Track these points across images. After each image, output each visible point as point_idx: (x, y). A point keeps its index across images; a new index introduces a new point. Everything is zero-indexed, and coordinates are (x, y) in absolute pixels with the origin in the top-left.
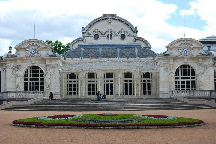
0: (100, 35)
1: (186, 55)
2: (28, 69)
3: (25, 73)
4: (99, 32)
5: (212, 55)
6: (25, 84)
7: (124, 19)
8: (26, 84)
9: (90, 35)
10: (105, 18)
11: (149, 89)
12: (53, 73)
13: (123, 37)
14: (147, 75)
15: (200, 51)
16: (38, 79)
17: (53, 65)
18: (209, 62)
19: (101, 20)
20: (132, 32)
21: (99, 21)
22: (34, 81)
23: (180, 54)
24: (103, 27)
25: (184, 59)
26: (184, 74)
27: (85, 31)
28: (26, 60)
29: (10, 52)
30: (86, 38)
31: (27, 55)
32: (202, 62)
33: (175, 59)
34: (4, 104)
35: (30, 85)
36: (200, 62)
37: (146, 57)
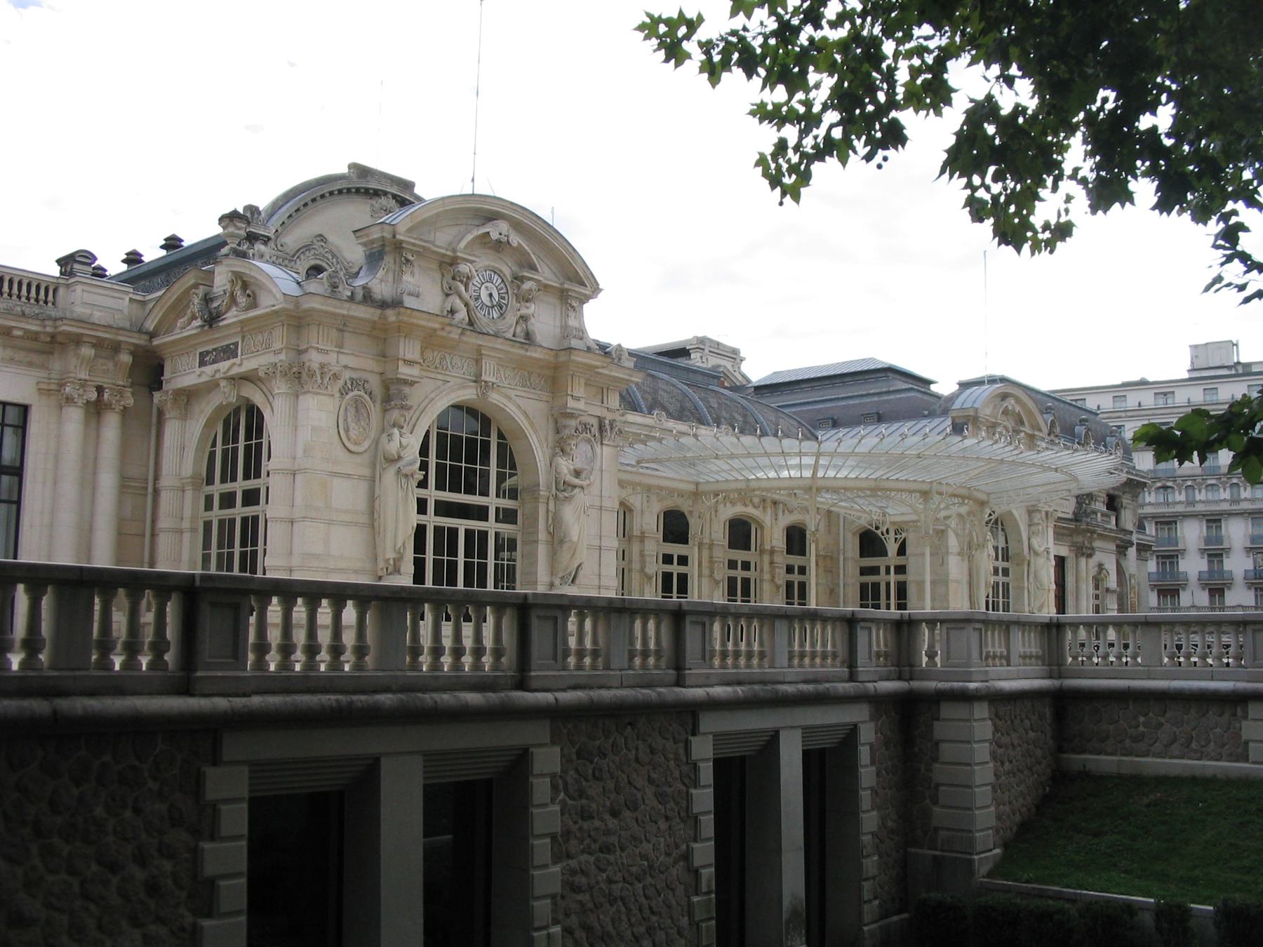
4: (334, 256)
16: (481, 513)
19: (349, 190)
21: (340, 192)
22: (462, 525)
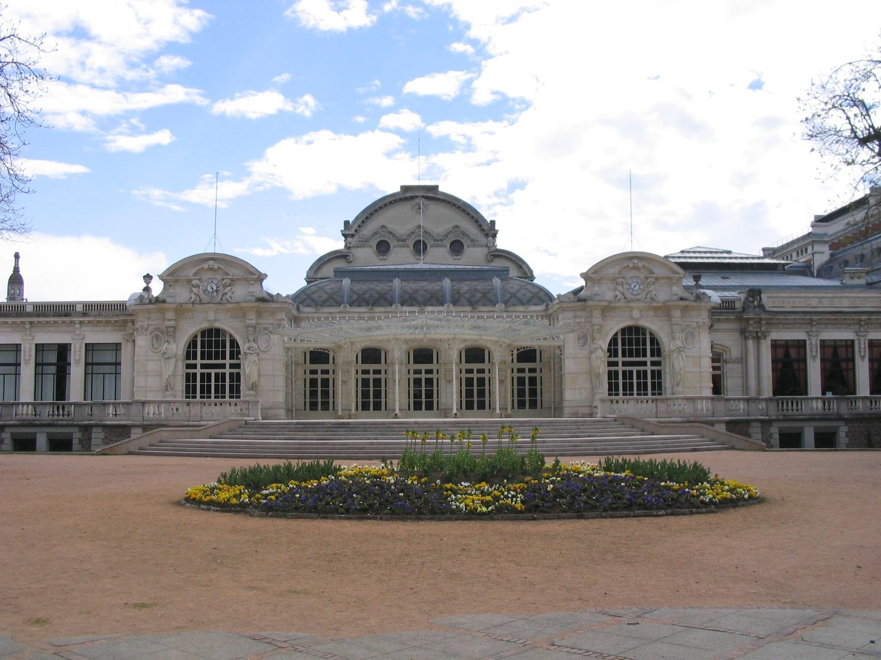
0: (392, 243)
1: (638, 300)
2: (196, 336)
3: (189, 347)
4: (390, 233)
5: (707, 300)
6: (188, 380)
7: (459, 200)
8: (190, 378)
9: (364, 243)
10: (409, 195)
11: (533, 393)
12: (267, 348)
13: (457, 247)
14: (527, 355)
16: (223, 366)
17: (267, 326)
19: (396, 201)
20: (483, 236)
24: (401, 222)
25: (631, 309)
26: (631, 351)
27: (352, 231)
28: (189, 310)
29: (147, 289)
30: (353, 251)
31: (194, 297)
33: (607, 309)
34: (133, 436)
35: (202, 380)
37: (523, 304)
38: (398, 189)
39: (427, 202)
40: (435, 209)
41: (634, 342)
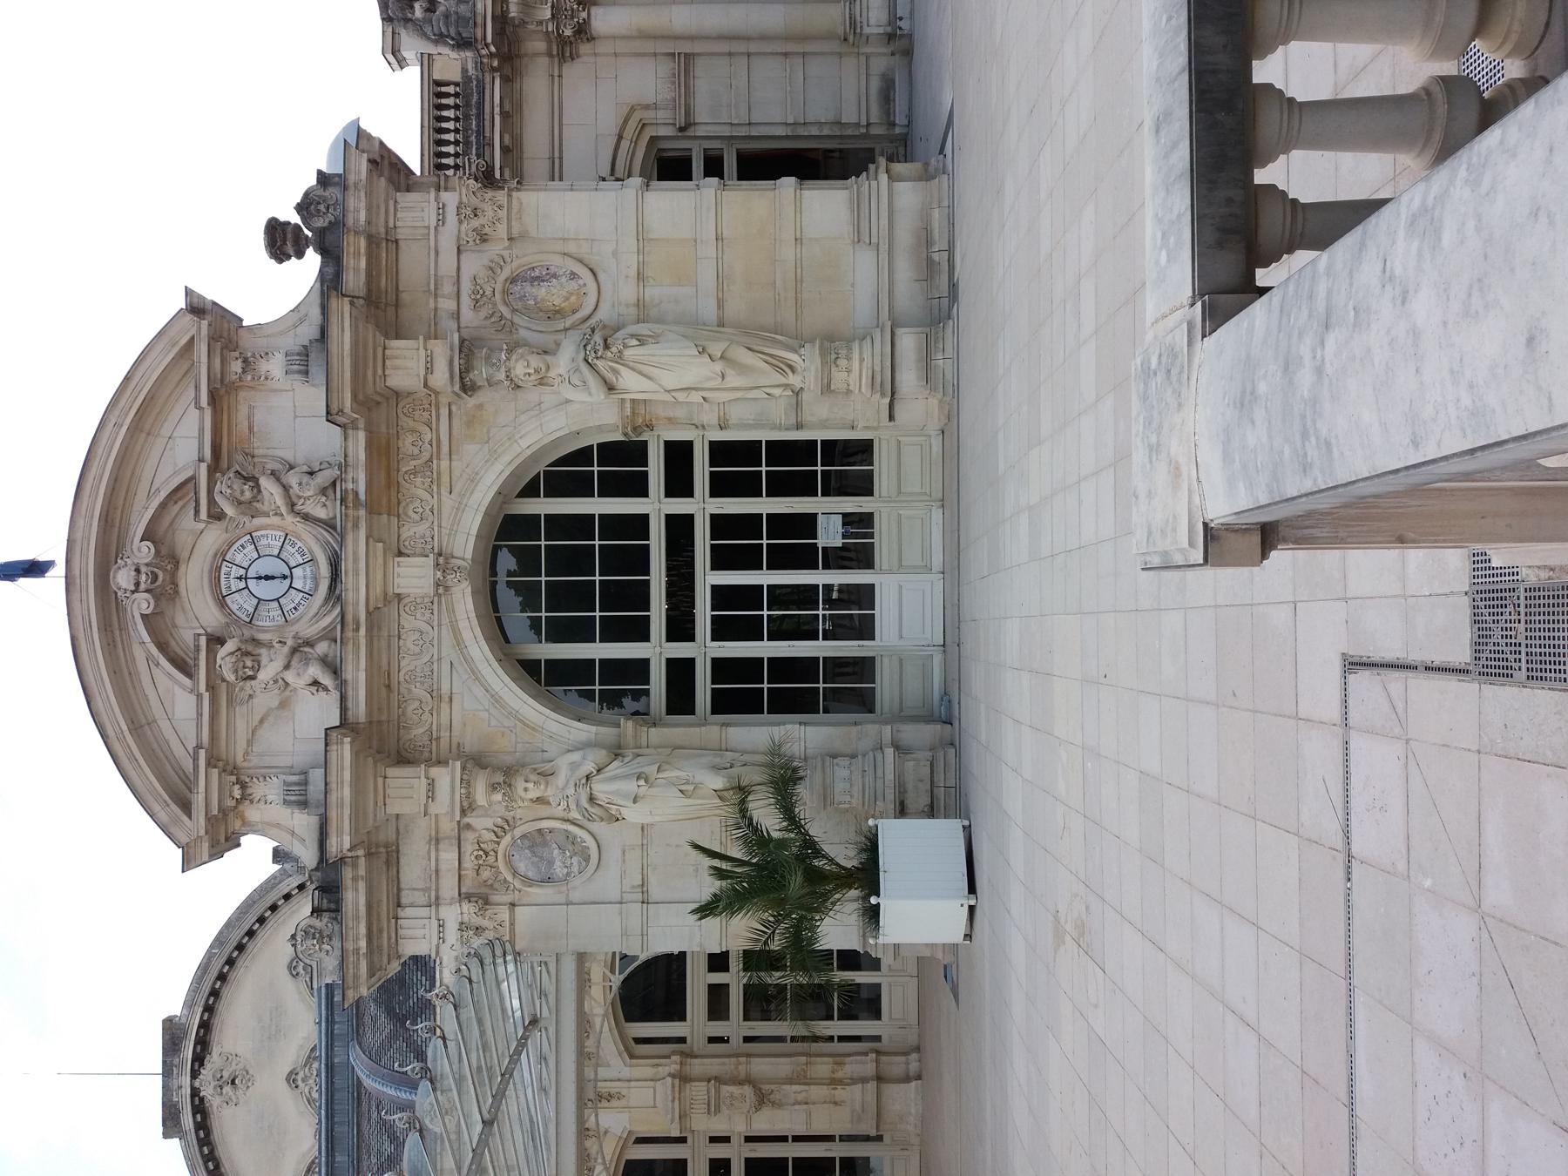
7: (209, 956)
15: (275, 367)
18: (447, 242)
23: (315, 671)
32: (440, 350)
36: (440, 378)
38: (175, 1143)
39: (214, 1061)
40: (236, 1034)
41: (575, 571)
